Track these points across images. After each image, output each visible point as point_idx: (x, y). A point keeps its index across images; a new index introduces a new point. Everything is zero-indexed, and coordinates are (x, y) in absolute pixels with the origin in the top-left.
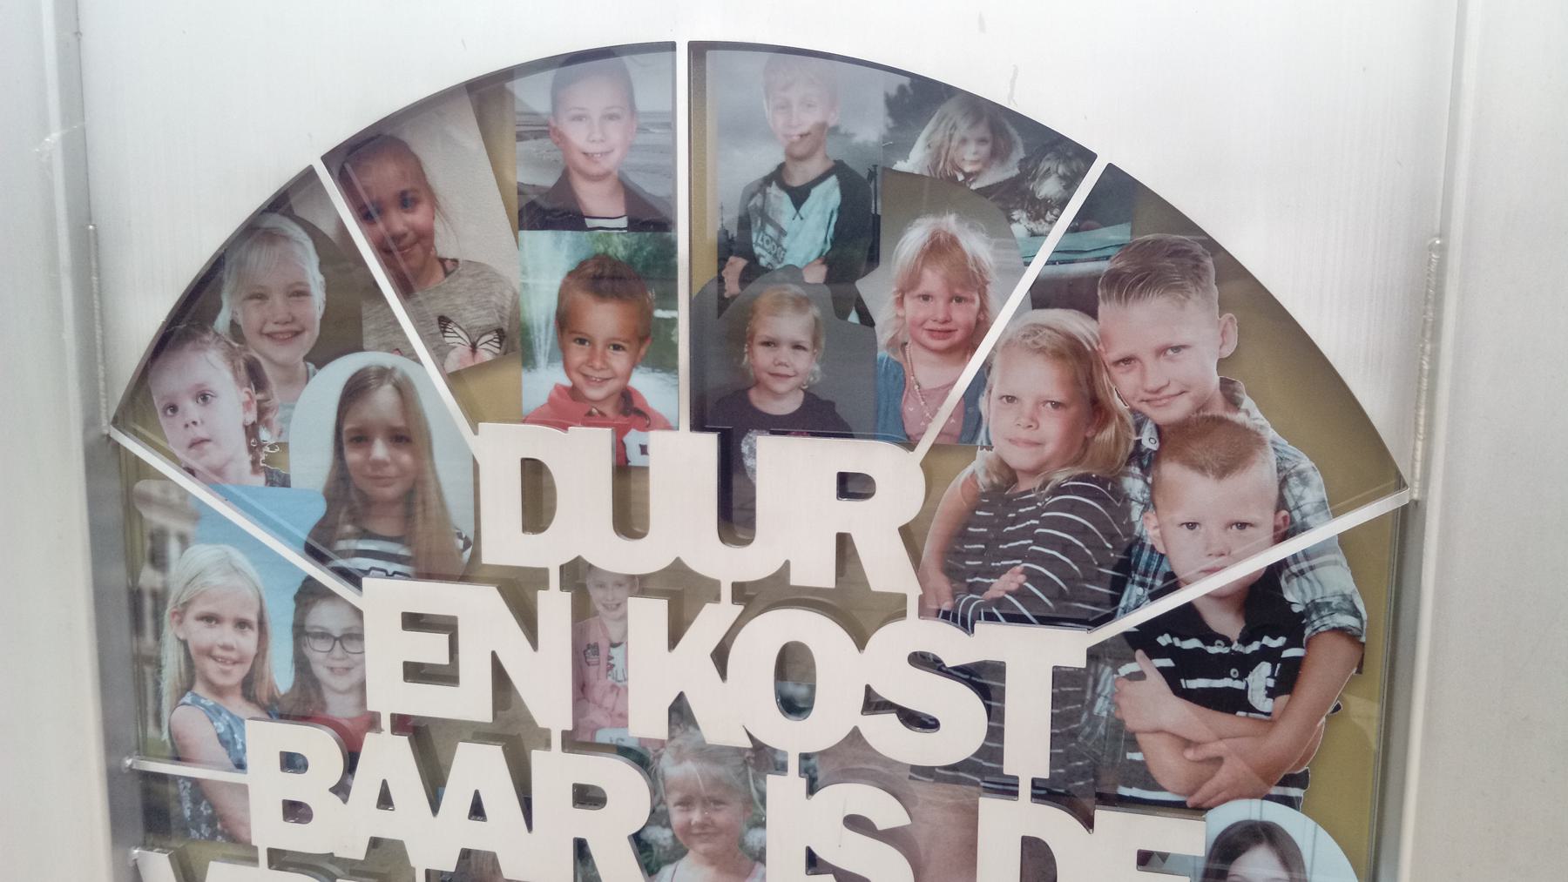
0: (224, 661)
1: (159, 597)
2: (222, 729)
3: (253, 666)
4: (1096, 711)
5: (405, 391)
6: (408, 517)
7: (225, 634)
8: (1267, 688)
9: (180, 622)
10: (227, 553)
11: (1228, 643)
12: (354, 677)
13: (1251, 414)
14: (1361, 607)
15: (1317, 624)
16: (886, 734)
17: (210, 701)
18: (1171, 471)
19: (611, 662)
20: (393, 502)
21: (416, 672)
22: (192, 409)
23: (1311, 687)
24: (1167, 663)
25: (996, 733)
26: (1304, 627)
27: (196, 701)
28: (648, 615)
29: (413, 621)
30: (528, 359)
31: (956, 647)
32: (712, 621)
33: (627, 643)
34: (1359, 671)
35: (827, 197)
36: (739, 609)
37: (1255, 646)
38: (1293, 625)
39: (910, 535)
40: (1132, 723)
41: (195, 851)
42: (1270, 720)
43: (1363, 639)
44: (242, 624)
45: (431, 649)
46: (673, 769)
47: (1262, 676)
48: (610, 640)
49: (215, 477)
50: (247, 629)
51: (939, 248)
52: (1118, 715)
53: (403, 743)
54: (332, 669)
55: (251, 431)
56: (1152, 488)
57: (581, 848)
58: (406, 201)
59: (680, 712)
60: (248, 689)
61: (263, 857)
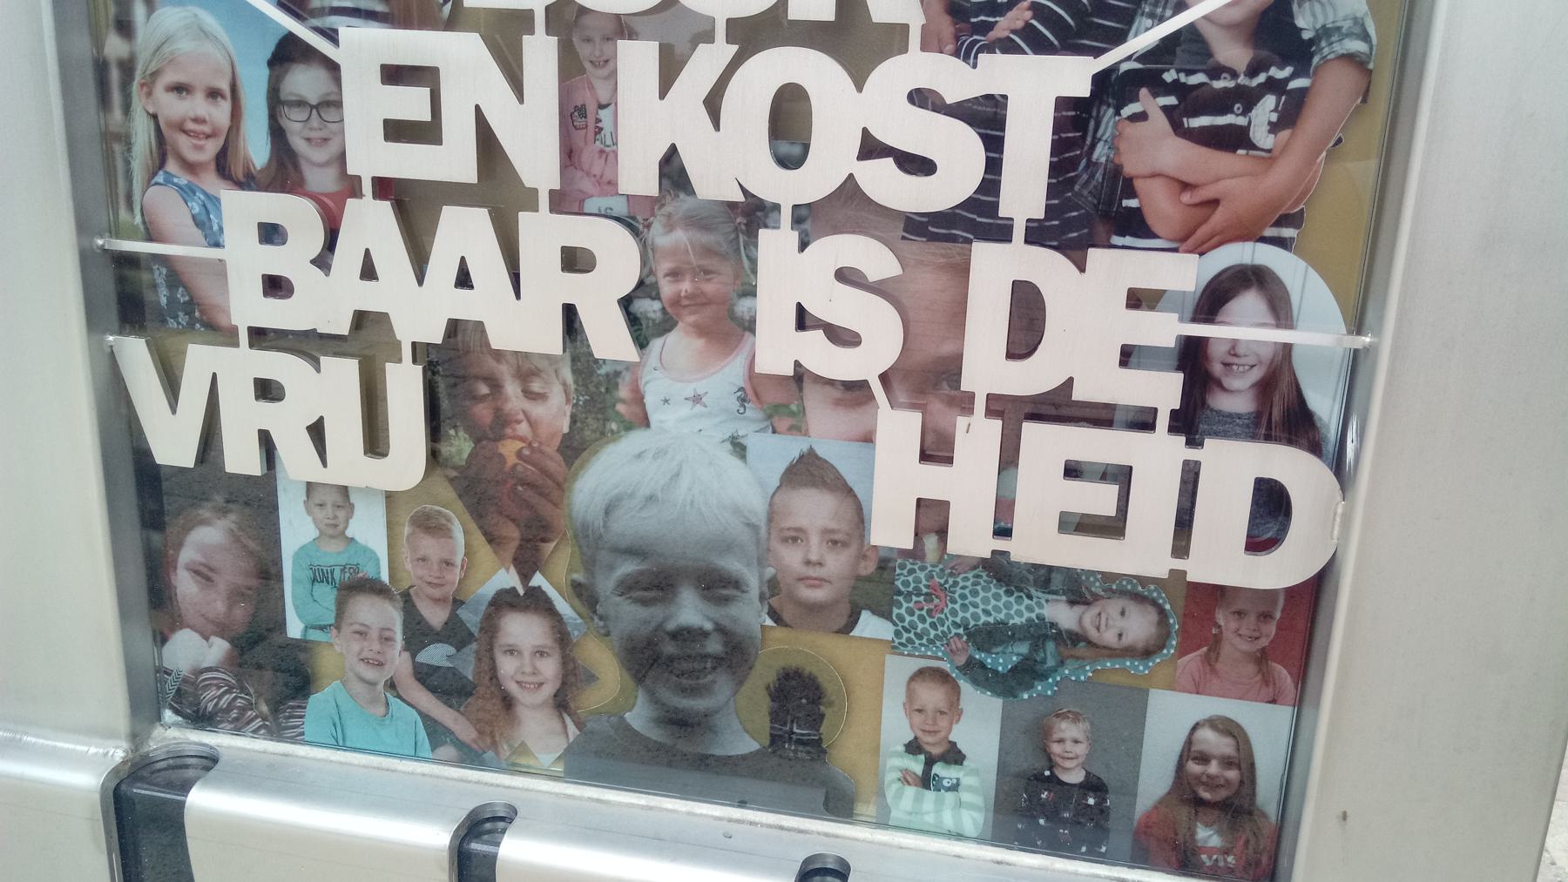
0: (196, 135)
1: (127, 67)
2: (197, 210)
3: (226, 141)
4: (1095, 156)
7: (197, 105)
8: (1270, 123)
9: (149, 94)
10: (196, 15)
11: (1234, 75)
14: (1372, 31)
15: (1326, 51)
17: (183, 179)
19: (600, 125)
21: (397, 131)
23: (1314, 120)
24: (1171, 100)
25: (994, 166)
26: (1312, 56)
27: (169, 180)
29: (394, 75)
33: (616, 104)
34: (1364, 101)
36: (734, 48)
37: (1262, 78)
38: (1299, 52)
40: (1129, 169)
41: (172, 343)
42: (1270, 157)
43: (1371, 66)
44: (214, 94)
45: (411, 104)
48: (598, 101)
50: (219, 99)
52: (1117, 161)
53: (386, 207)
54: (308, 140)
57: (570, 312)
60: (224, 165)
61: (244, 337)
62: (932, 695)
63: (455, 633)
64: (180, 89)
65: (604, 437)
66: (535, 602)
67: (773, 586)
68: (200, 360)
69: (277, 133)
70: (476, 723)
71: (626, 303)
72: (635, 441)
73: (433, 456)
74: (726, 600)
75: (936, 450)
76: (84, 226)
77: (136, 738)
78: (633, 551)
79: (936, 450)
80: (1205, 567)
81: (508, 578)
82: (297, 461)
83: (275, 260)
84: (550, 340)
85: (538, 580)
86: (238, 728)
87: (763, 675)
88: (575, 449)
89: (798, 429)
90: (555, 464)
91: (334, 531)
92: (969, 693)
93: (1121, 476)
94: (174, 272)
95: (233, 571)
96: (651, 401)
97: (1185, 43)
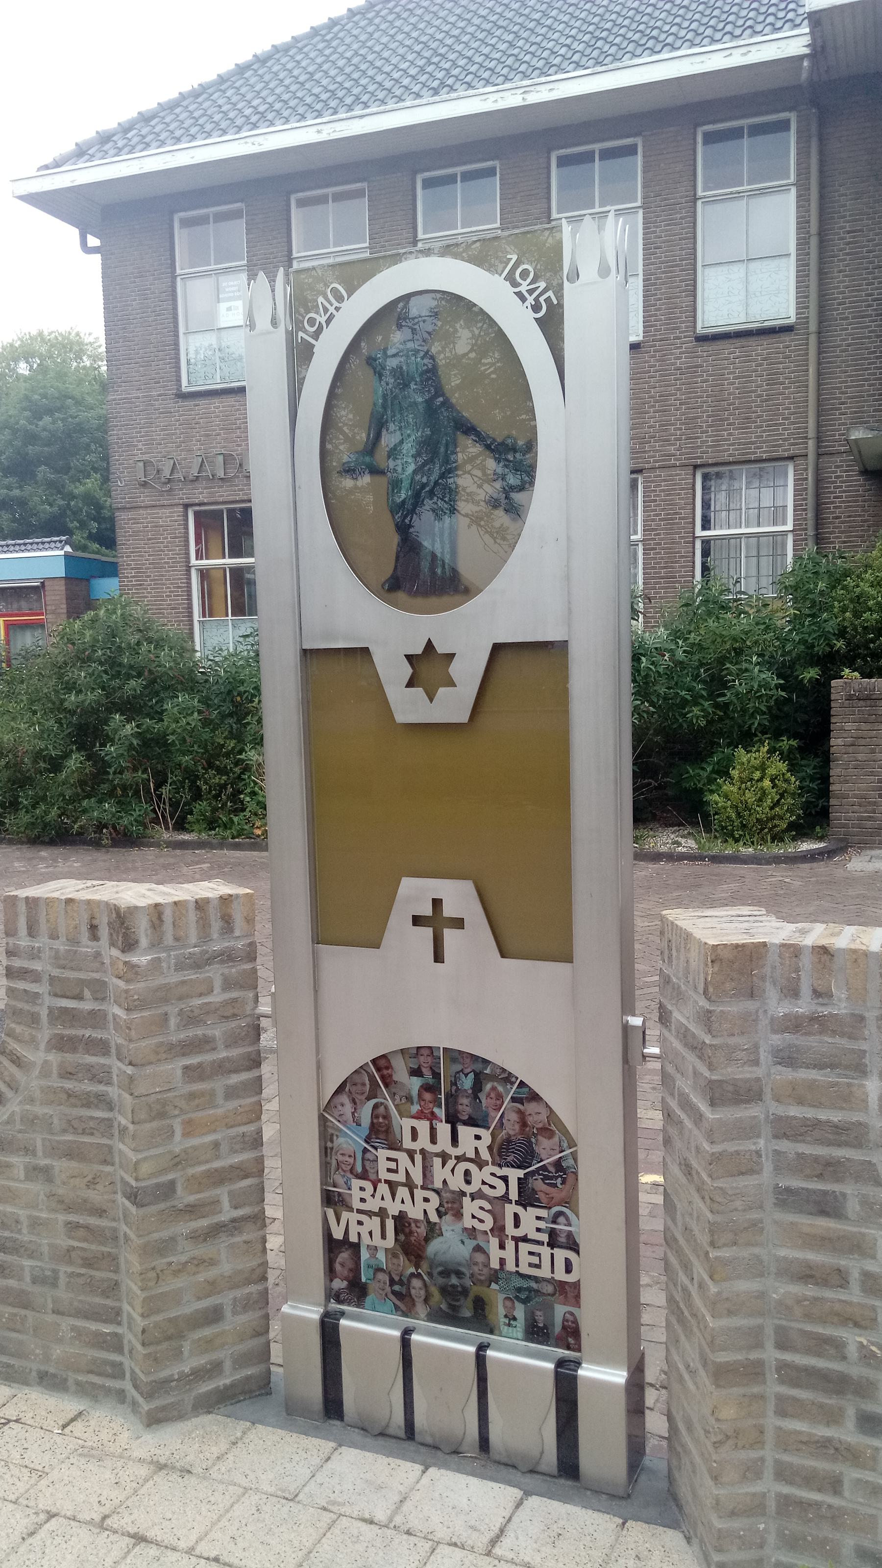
1: (332, 1149)
5: (386, 1108)
6: (387, 1136)
7: (347, 1159)
12: (375, 1170)
16: (486, 1189)
17: (342, 1173)
18: (540, 1138)
20: (383, 1132)
21: (389, 1170)
22: (340, 1108)
25: (507, 1189)
28: (438, 1161)
29: (388, 1159)
30: (412, 1103)
31: (500, 1172)
32: (451, 1163)
35: (472, 1076)
39: (490, 1148)
40: (536, 1189)
44: (350, 1156)
45: (393, 1165)
46: (443, 1194)
47: (559, 1180)
49: (344, 1123)
51: (494, 1089)
55: (353, 1114)
56: (537, 1141)
57: (425, 1211)
58: (387, 1068)
59: (445, 1182)
62: (508, 1303)
63: (401, 1282)
64: (343, 1154)
66: (419, 1276)
67: (472, 1275)
68: (345, 1215)
70: (406, 1306)
71: (437, 1210)
72: (440, 1239)
73: (396, 1240)
74: (462, 1278)
75: (502, 1247)
76: (322, 1184)
77: (326, 1306)
78: (440, 1265)
79: (502, 1247)
81: (412, 1270)
82: (366, 1240)
83: (363, 1195)
84: (421, 1216)
85: (419, 1271)
86: (349, 1305)
87: (471, 1296)
88: (427, 1240)
89: (475, 1238)
90: (423, 1243)
91: (373, 1256)
92: (517, 1304)
93: (539, 1255)
94: (339, 1194)
95: (350, 1264)
96: (443, 1230)
97: (543, 1167)
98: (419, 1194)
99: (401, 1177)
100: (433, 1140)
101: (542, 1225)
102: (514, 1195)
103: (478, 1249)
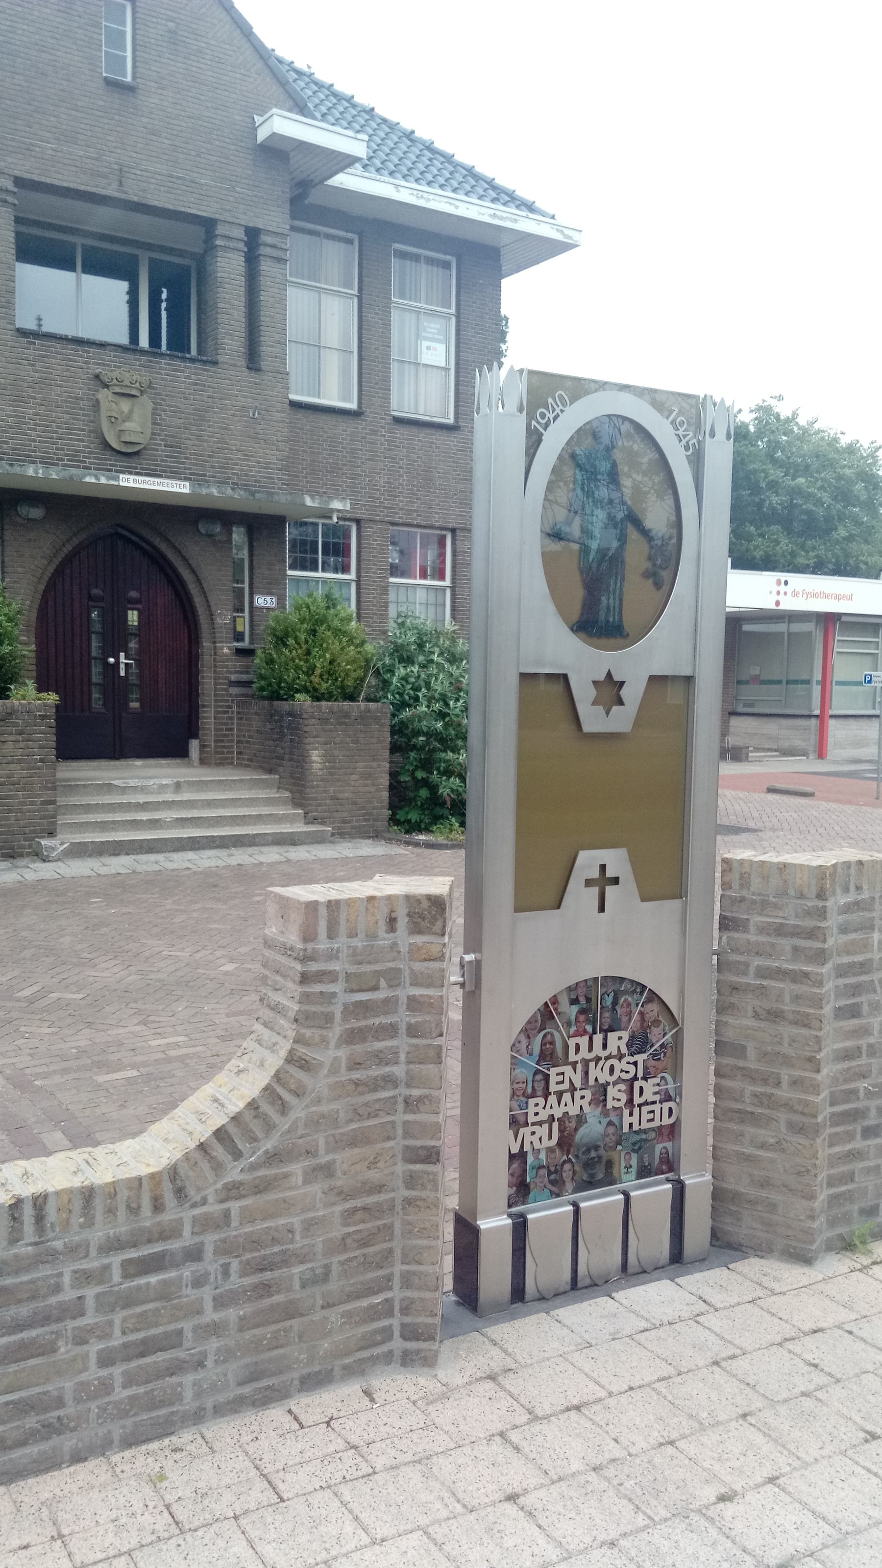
5: (552, 1035)
6: (551, 1058)
13: (660, 1018)
21: (557, 1083)
29: (558, 1074)
35: (612, 994)
45: (560, 1078)
51: (626, 1000)
55: (527, 1047)
59: (596, 1080)
60: (523, 1095)
62: (627, 1157)
63: (556, 1172)
65: (581, 1126)
66: (570, 1160)
69: (533, 1087)
72: (585, 1126)
75: (631, 1114)
78: (583, 1146)
79: (631, 1114)
80: (663, 1123)
83: (537, 1109)
86: (516, 1206)
87: (604, 1162)
98: (578, 1094)
99: (566, 1086)
100: (590, 1049)
101: (657, 1089)
102: (640, 1074)
103: (610, 1123)
